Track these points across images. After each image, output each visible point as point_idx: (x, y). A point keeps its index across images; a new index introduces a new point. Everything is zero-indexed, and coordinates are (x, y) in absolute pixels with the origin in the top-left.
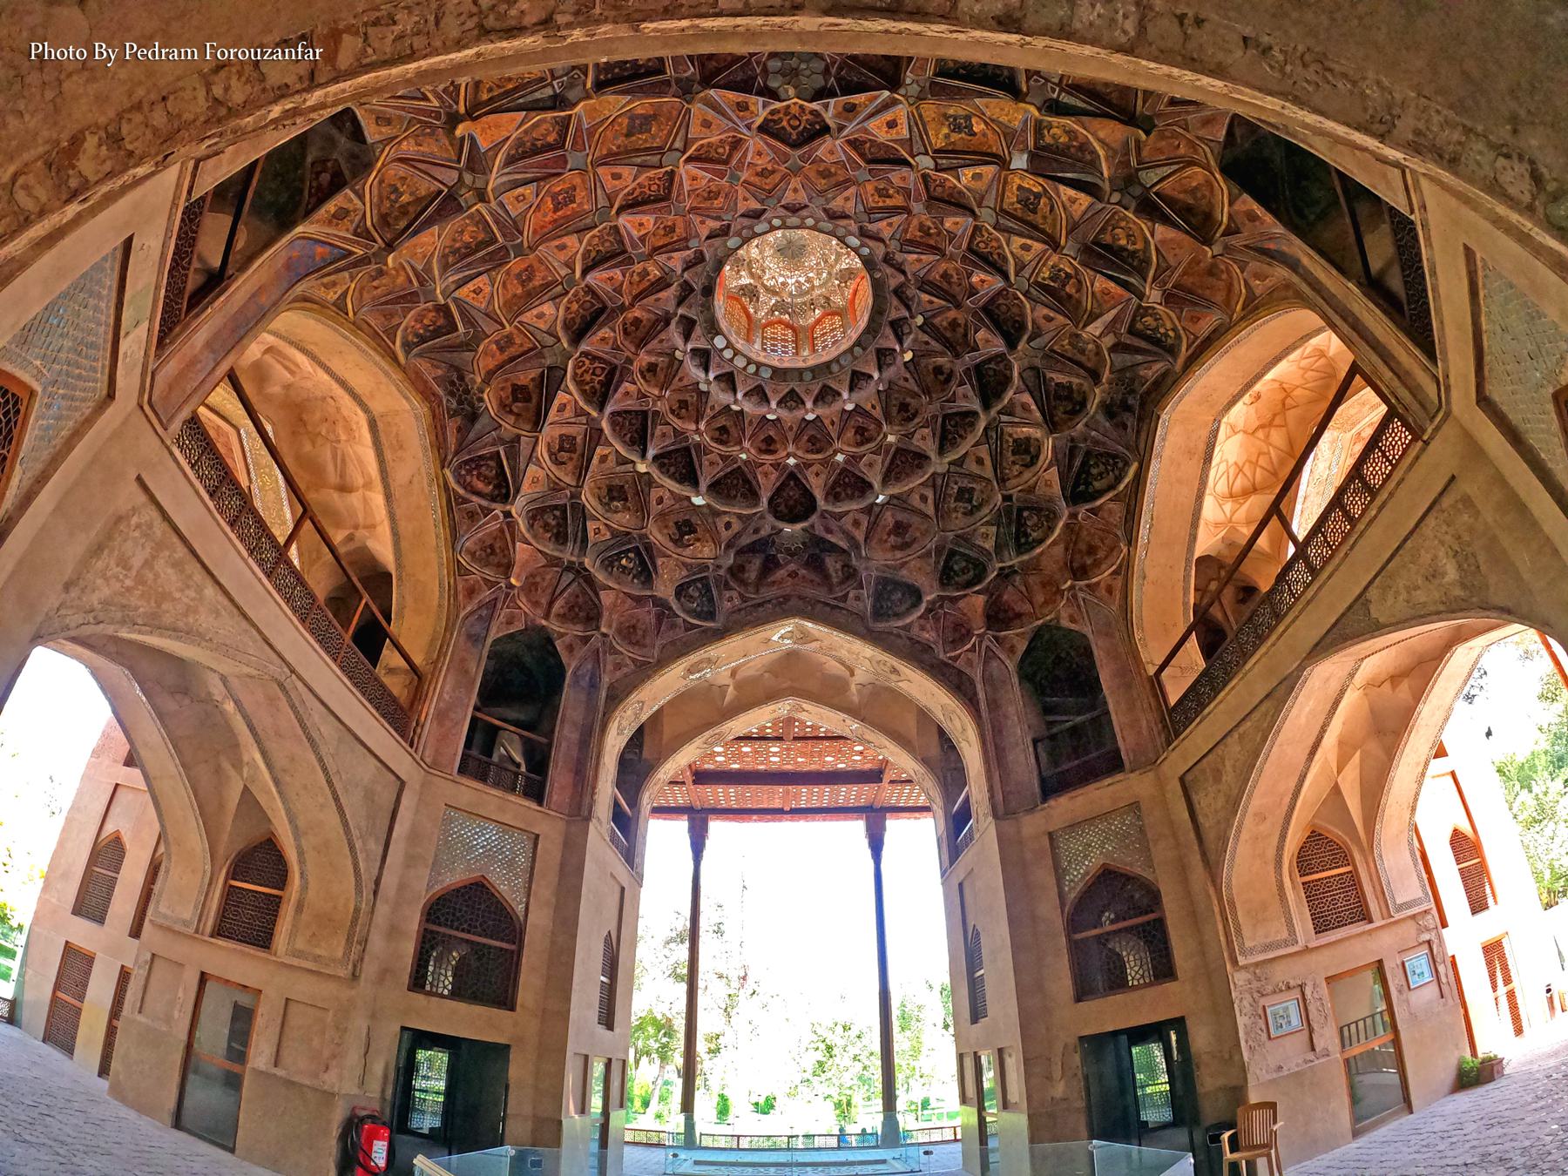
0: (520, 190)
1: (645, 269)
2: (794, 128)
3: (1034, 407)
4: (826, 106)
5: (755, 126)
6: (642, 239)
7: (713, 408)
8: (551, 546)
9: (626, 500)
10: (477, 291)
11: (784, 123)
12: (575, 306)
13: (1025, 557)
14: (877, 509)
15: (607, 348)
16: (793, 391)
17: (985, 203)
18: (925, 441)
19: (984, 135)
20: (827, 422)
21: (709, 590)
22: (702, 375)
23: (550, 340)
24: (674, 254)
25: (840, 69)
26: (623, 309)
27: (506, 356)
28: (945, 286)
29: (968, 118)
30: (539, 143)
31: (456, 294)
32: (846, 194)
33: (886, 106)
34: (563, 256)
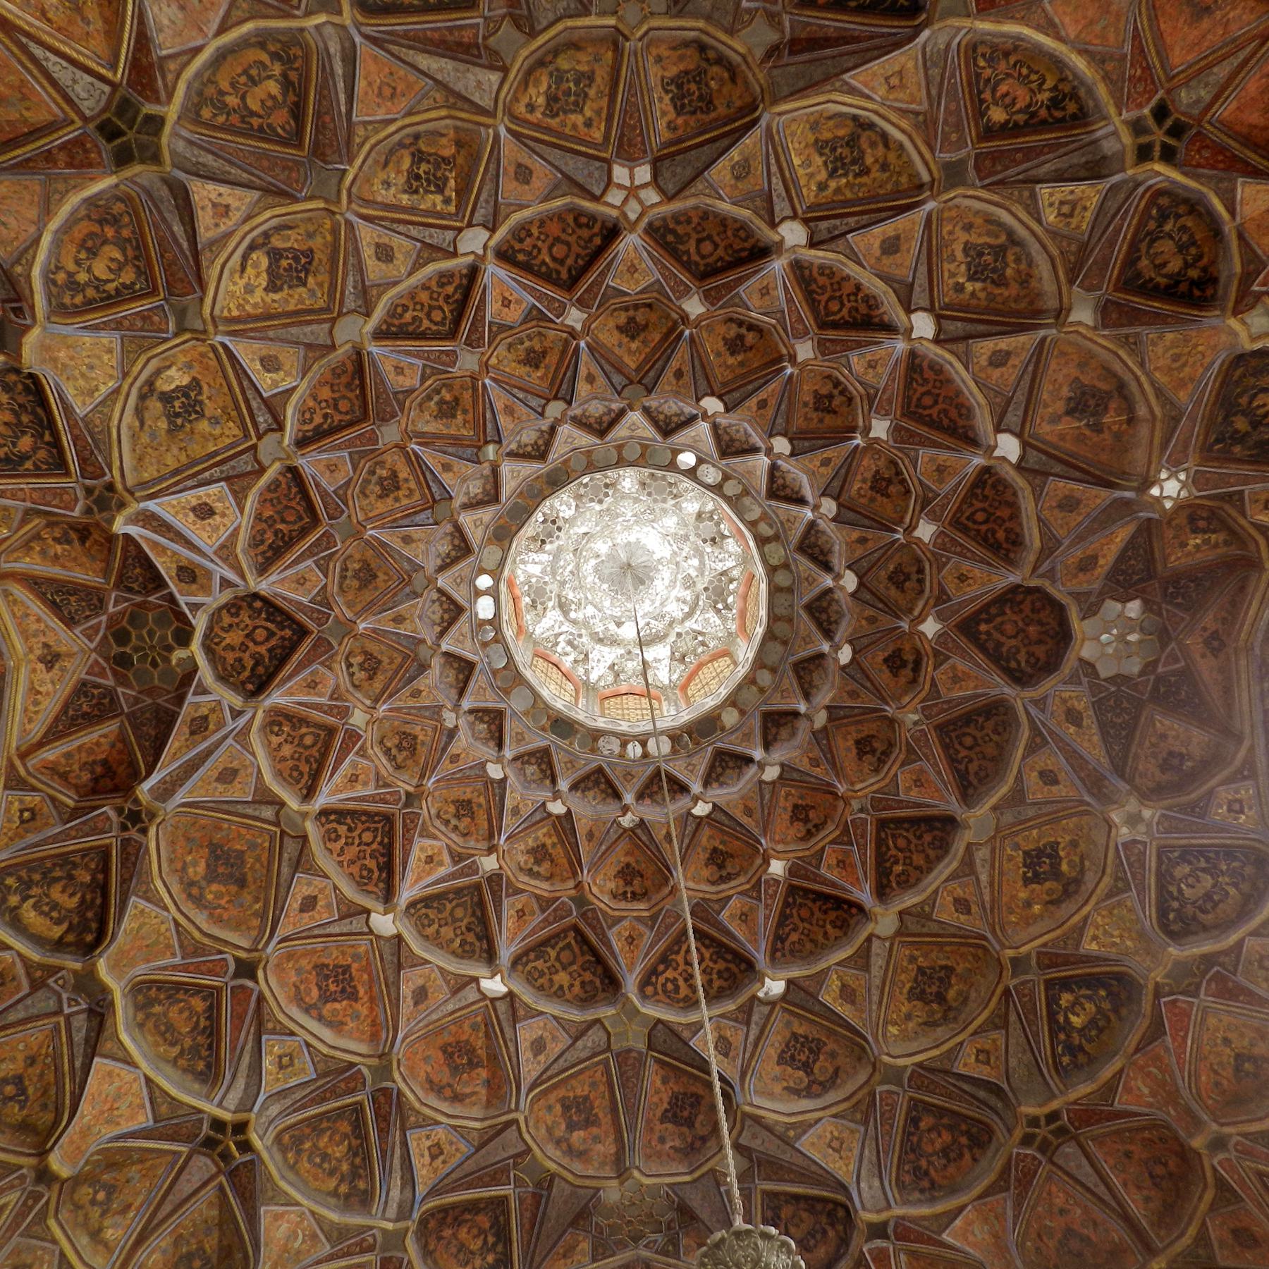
0: (268, 1063)
1: (531, 851)
2: (271, 634)
3: (735, 154)
4: (195, 607)
5: (237, 701)
6: (457, 857)
7: (815, 763)
8: (984, 1163)
9: (949, 970)
10: (436, 1151)
11: (262, 650)
12: (562, 978)
13: (1102, 91)
14: (1034, 458)
15: (648, 936)
16: (809, 608)
17: (323, 339)
18: (872, 364)
19: (189, 366)
20: (859, 552)
21: (1202, 852)
22: (753, 769)
23: (594, 1038)
24: (508, 804)
25: (130, 590)
26: (581, 901)
27: (606, 1120)
28: (552, 359)
29: (166, 398)
30: (203, 1023)
31: (421, 1190)
32: (396, 544)
33: (163, 527)
34: (439, 992)
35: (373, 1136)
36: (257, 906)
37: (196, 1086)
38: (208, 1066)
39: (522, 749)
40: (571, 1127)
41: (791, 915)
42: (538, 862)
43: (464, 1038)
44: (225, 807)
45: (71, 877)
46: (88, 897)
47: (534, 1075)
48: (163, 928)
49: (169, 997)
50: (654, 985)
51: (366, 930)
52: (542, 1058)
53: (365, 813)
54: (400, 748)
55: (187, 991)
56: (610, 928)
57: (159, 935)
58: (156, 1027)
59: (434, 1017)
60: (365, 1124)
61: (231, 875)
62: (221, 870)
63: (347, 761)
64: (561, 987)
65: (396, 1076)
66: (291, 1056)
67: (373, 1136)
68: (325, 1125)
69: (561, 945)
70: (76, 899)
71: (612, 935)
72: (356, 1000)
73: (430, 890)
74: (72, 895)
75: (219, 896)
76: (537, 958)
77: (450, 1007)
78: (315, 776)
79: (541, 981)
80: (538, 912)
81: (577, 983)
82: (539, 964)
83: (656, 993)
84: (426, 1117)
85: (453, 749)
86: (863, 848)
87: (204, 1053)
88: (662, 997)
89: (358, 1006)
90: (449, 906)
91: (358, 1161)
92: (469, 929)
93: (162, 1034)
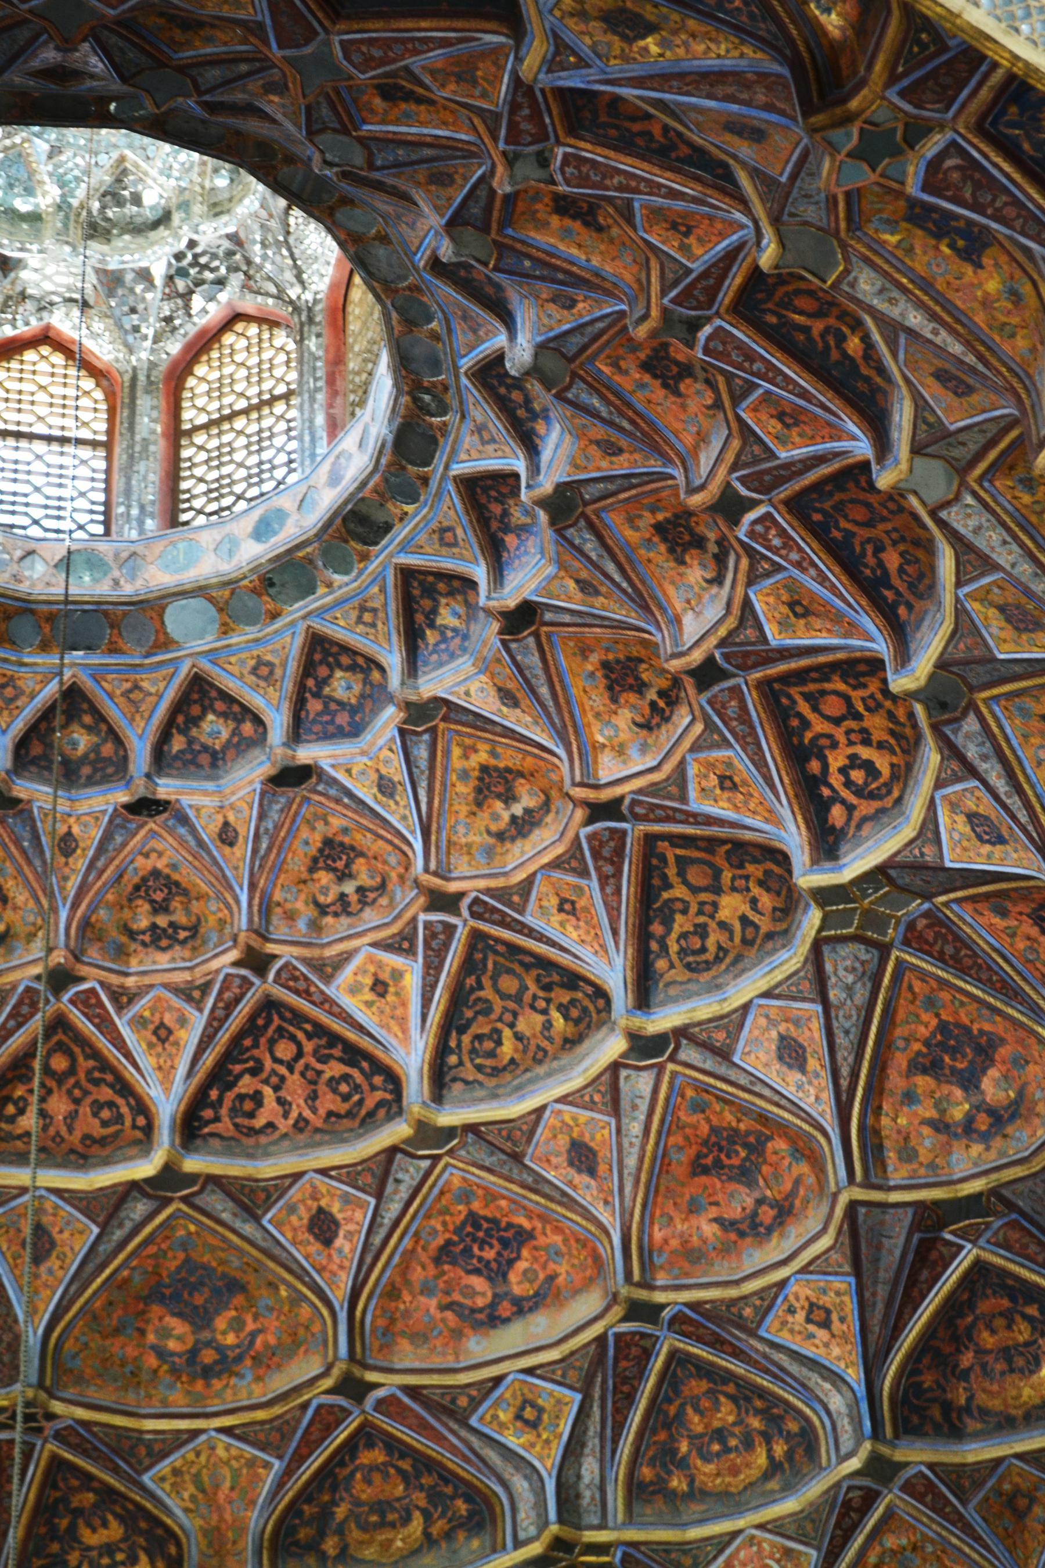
0: (512, 1441)
10: (819, 1316)
12: (731, 906)
24: (366, 793)
31: (855, 1375)
35: (738, 1368)
36: (284, 1293)
37: (475, 1543)
38: (468, 1499)
39: (289, 685)
40: (970, 1082)
41: (849, 535)
42: (509, 798)
43: (705, 1129)
44: (90, 1267)
45: (78, 1512)
46: (118, 1510)
47: (828, 1096)
48: (221, 1452)
49: (334, 1489)
50: (836, 798)
51: (425, 1164)
52: (812, 1064)
53: (236, 1040)
54: (160, 908)
55: (342, 1464)
56: (684, 798)
57: (227, 1463)
58: (364, 1527)
59: (631, 1162)
60: (712, 1364)
61: (216, 1292)
62: (199, 1300)
63: (125, 1032)
64: (744, 920)
65: (660, 1297)
66: (526, 1402)
67: (738, 1368)
68: (672, 1410)
69: (671, 872)
70: (114, 1524)
71: (697, 804)
72: (530, 1235)
73: (435, 1015)
74: (105, 1524)
75: (237, 1325)
76: (668, 923)
77: (635, 1128)
78: (125, 1088)
79: (711, 942)
80: (583, 882)
81: (756, 891)
82: (681, 923)
83: (850, 808)
84: (760, 1293)
85: (208, 829)
86: (771, 374)
87: (449, 1490)
88: (866, 807)
89: (542, 1240)
90: (488, 993)
91: (758, 1404)
92: (547, 988)
93: (383, 1524)
